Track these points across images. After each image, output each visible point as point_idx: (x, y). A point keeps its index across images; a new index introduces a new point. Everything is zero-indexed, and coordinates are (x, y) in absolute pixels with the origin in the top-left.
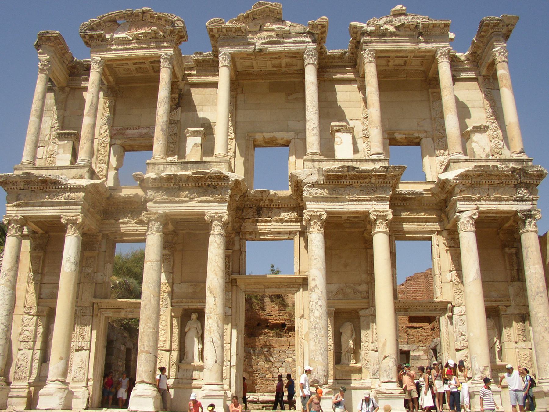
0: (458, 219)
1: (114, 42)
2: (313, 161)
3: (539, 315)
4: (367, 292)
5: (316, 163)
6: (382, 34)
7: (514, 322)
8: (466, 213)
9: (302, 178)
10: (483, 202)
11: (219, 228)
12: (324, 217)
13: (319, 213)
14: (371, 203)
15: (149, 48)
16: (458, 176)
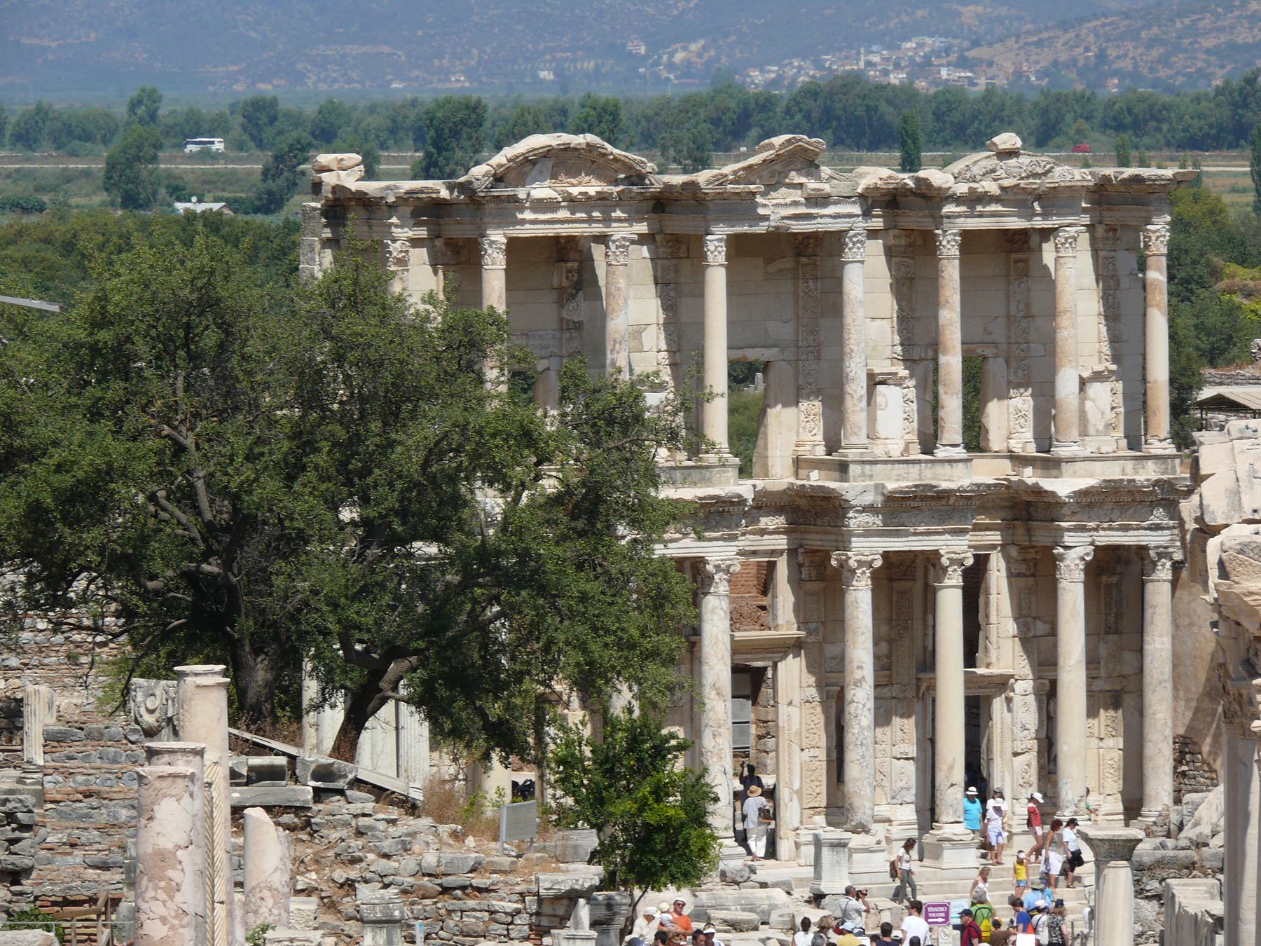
0: (1061, 558)
1: (528, 205)
2: (863, 462)
3: (1159, 716)
4: (889, 656)
5: (867, 467)
6: (974, 200)
7: (1102, 711)
8: (1076, 551)
9: (848, 497)
10: (1102, 533)
11: (726, 583)
12: (878, 563)
13: (871, 557)
14: (943, 537)
15: (590, 220)
16: (1075, 492)
